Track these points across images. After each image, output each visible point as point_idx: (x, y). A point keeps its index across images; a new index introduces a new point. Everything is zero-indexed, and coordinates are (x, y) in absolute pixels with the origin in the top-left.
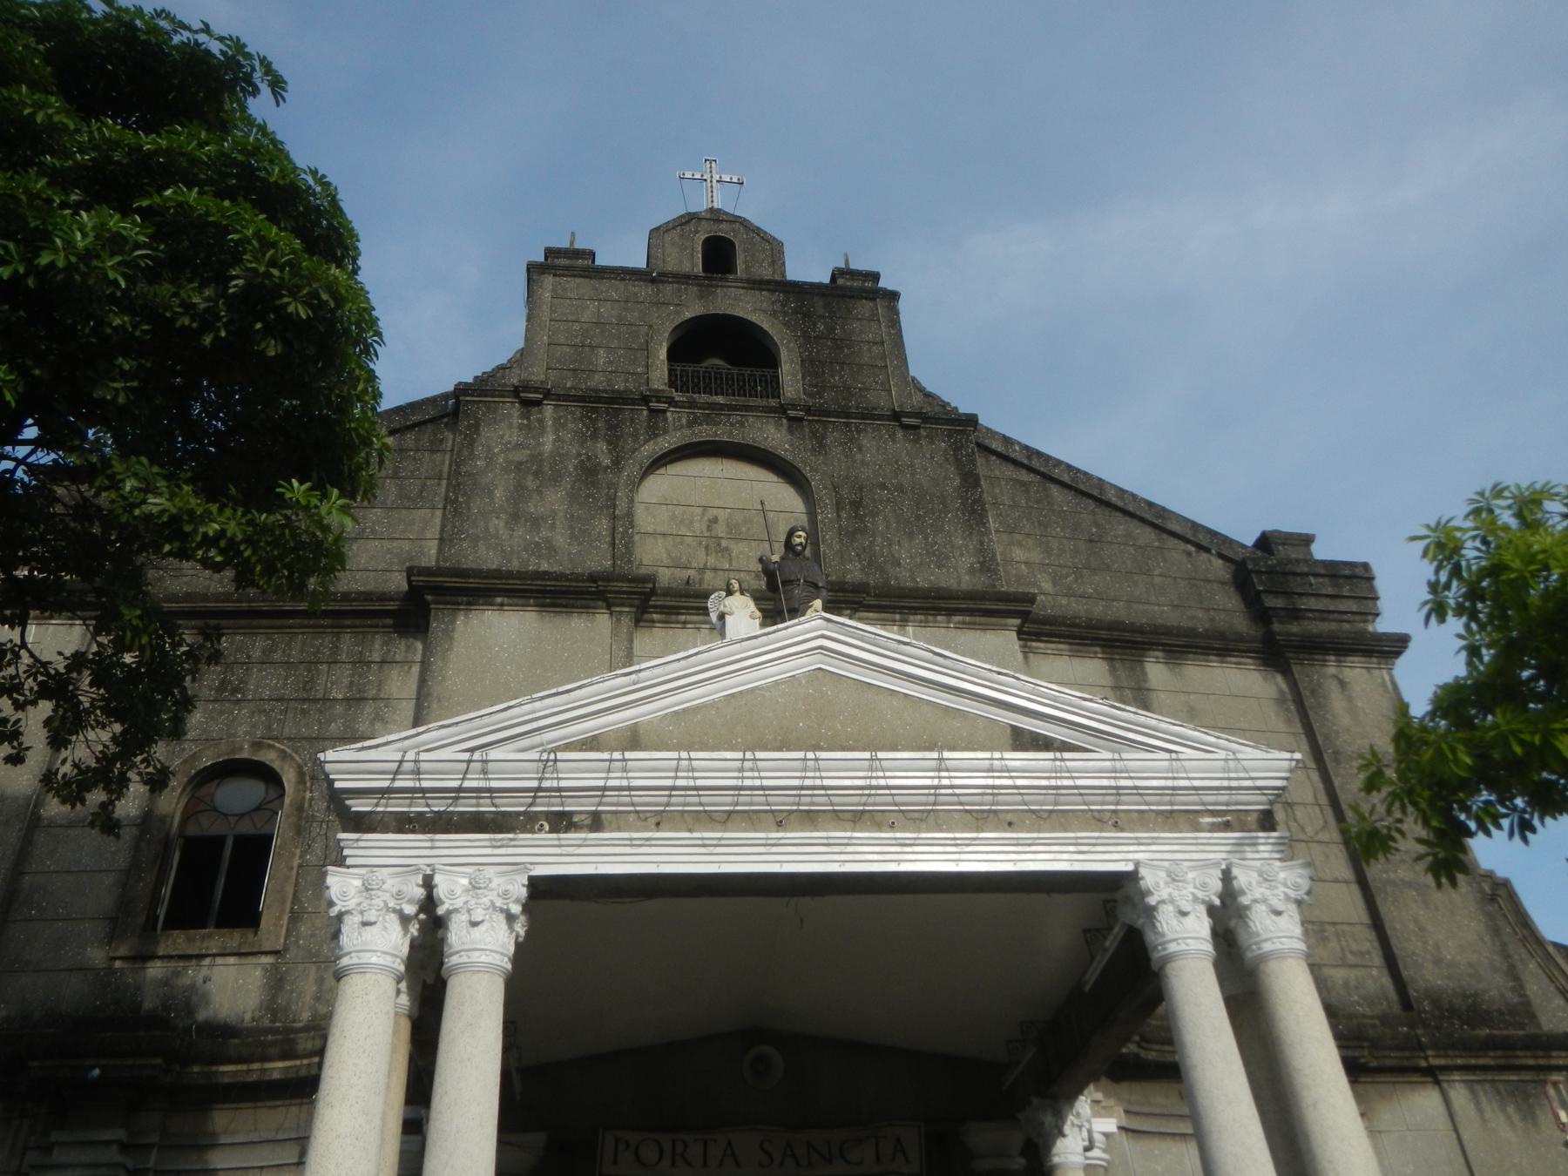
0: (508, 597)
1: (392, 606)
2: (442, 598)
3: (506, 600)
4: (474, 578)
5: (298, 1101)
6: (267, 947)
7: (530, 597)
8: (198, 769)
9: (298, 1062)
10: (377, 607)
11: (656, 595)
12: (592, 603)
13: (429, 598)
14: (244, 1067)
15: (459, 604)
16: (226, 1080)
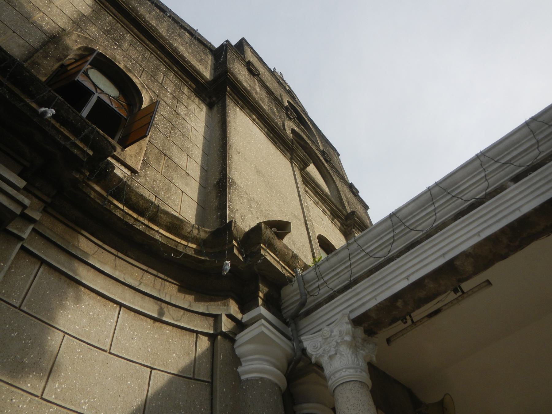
0: (258, 119)
1: (202, 81)
2: (233, 95)
3: (257, 120)
4: (251, 98)
5: (155, 272)
6: (130, 163)
7: (266, 127)
8: (93, 47)
9: (178, 240)
10: (194, 74)
11: (304, 171)
12: (286, 152)
13: (228, 89)
14: (135, 216)
15: (238, 103)
16: (118, 213)
